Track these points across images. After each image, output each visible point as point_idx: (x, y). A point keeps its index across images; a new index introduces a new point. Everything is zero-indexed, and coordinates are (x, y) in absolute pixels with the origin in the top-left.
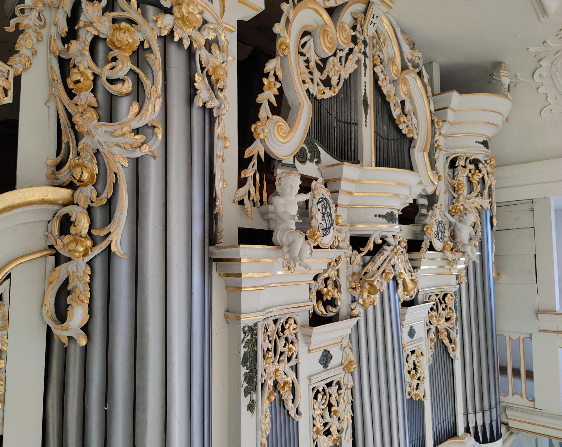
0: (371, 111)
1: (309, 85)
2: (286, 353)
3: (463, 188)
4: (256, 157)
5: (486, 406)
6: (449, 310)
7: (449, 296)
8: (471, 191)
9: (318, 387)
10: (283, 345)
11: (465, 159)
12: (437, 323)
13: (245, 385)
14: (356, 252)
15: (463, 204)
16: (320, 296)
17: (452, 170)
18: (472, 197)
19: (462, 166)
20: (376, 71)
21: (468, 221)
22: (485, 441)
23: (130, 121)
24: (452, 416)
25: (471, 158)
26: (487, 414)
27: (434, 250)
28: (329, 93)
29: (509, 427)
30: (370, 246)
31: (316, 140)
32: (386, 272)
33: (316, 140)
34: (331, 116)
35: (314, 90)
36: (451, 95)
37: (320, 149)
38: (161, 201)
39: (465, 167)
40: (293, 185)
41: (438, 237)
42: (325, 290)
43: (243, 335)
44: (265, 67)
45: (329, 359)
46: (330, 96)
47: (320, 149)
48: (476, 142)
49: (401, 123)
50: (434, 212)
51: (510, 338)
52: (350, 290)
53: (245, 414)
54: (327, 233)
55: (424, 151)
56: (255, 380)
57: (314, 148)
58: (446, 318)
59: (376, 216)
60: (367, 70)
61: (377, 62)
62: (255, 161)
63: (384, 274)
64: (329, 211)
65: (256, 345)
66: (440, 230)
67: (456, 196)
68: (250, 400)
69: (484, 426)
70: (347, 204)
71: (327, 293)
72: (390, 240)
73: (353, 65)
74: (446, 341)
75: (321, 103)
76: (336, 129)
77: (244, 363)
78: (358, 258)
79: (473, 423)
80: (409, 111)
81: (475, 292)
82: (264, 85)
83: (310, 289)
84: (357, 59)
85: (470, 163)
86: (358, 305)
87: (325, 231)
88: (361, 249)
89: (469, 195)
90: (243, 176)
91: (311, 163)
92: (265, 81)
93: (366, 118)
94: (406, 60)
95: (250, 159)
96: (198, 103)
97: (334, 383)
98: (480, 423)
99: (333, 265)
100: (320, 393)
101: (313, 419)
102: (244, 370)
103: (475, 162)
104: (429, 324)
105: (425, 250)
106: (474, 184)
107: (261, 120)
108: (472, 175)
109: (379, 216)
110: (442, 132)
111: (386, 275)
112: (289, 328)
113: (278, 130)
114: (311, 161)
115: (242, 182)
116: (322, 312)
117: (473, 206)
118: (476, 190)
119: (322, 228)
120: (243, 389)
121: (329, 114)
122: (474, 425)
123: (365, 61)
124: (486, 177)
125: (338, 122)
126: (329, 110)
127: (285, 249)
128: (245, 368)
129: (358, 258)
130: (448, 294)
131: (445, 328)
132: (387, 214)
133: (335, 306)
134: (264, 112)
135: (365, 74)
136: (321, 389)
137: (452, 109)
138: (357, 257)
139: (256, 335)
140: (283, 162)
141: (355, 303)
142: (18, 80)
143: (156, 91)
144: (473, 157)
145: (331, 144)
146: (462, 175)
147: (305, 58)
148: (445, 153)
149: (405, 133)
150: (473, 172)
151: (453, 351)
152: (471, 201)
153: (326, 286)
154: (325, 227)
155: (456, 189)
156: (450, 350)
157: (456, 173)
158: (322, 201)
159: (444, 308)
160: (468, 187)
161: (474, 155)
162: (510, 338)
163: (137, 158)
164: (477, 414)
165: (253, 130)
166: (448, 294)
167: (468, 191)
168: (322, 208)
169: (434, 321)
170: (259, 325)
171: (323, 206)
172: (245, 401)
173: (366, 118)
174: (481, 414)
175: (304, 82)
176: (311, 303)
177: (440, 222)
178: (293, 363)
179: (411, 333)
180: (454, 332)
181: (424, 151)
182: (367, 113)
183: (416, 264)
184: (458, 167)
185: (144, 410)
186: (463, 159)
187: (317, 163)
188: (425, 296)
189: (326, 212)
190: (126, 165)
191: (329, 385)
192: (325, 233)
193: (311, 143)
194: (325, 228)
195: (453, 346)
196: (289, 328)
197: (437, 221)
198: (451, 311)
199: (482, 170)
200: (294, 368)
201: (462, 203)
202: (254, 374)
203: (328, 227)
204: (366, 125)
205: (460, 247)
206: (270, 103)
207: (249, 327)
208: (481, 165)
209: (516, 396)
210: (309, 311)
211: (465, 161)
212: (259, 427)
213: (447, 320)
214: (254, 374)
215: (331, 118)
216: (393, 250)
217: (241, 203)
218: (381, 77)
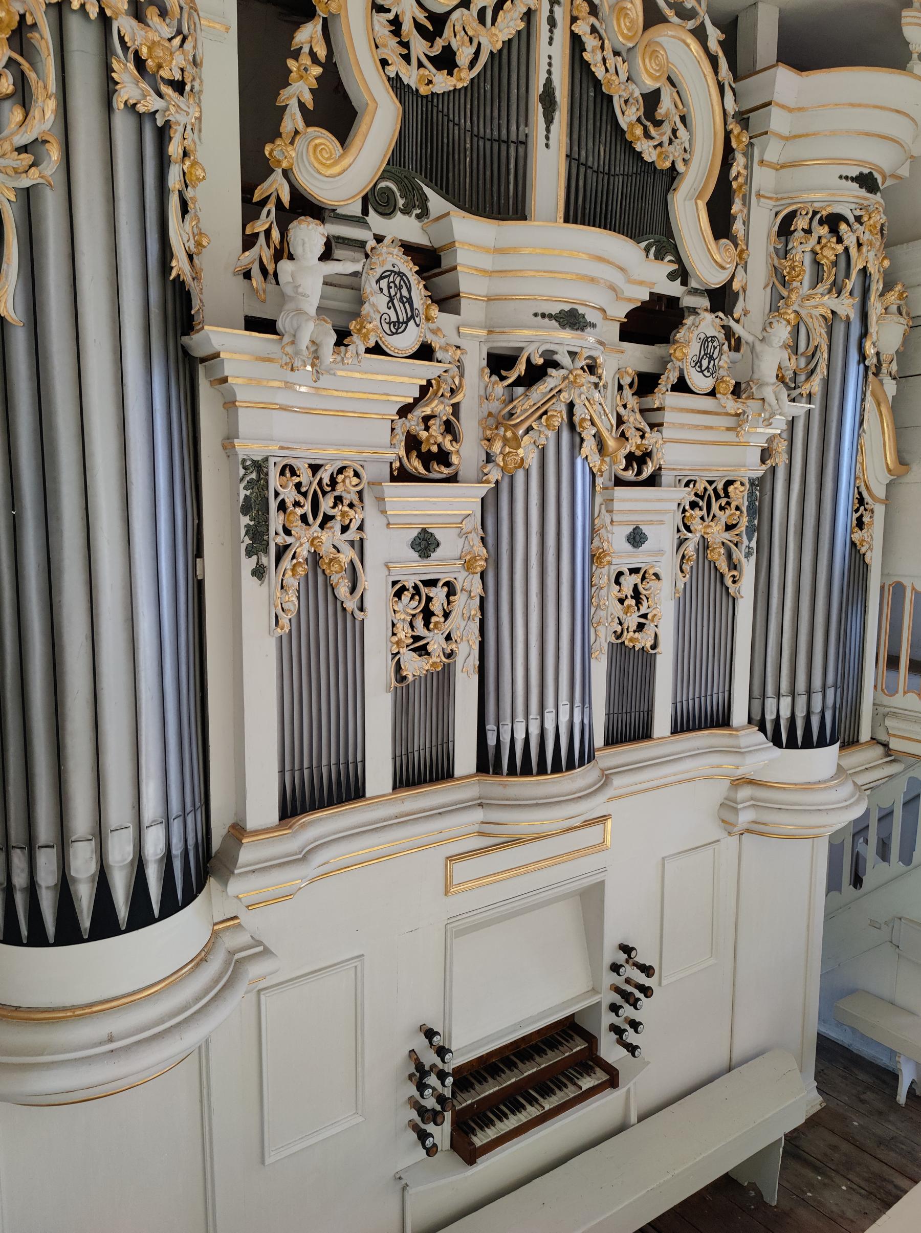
0: (561, 116)
1: (397, 67)
2: (338, 518)
3: (800, 277)
4: (273, 200)
5: (801, 686)
6: (733, 511)
7: (737, 484)
8: (817, 280)
9: (404, 581)
10: (332, 504)
11: (810, 215)
12: (703, 531)
13: (248, 541)
14: (495, 378)
15: (798, 309)
16: (412, 443)
17: (783, 239)
18: (816, 294)
19: (803, 230)
20: (576, 31)
21: (773, 338)
22: (792, 744)
23: (12, 134)
24: (724, 692)
25: (824, 213)
26: (801, 701)
27: (689, 391)
28: (443, 83)
29: (889, 749)
30: (521, 368)
31: (421, 174)
32: (549, 414)
33: (421, 174)
34: (456, 128)
35: (411, 76)
36: (776, 72)
37: (426, 190)
38: (65, 249)
39: (808, 232)
40: (306, 240)
41: (700, 367)
42: (424, 434)
43: (242, 472)
44: (293, 38)
45: (432, 547)
46: (452, 88)
47: (426, 190)
48: (841, 177)
49: (639, 139)
50: (697, 320)
51: (913, 588)
52: (483, 443)
53: (248, 582)
54: (400, 330)
55: (699, 197)
56: (265, 537)
57: (413, 189)
58: (726, 525)
59: (536, 315)
60: (558, 32)
61: (581, 11)
62: (271, 206)
63: (545, 417)
64: (405, 292)
65: (267, 489)
66: (706, 354)
67: (785, 293)
68: (257, 564)
69: (792, 720)
70: (484, 293)
71: (428, 439)
72: (565, 360)
73: (512, 24)
74: (723, 566)
75: (432, 102)
76: (468, 153)
77: (246, 509)
78: (499, 389)
79: (772, 712)
80: (667, 114)
81: (801, 481)
82: (290, 72)
83: (393, 429)
84: (525, 10)
85: (821, 222)
86: (496, 467)
87: (394, 326)
88: (504, 373)
89: (811, 292)
90: (248, 232)
91: (406, 217)
92: (292, 64)
93: (548, 130)
95: (264, 202)
96: (118, 104)
97: (440, 584)
98: (785, 713)
99: (442, 395)
100: (408, 590)
101: (393, 625)
102: (245, 520)
103: (833, 222)
104: (682, 529)
105: (665, 389)
106: (825, 268)
107: (284, 135)
108: (822, 249)
109: (543, 316)
110: (766, 158)
111: (547, 419)
112: (344, 481)
113: (315, 151)
114: (406, 211)
115: (249, 242)
116: (416, 469)
117: (816, 312)
118: (828, 278)
119: (387, 321)
120: (243, 547)
121: (451, 124)
122: (774, 716)
123: (551, 11)
124: (853, 251)
125: (475, 139)
126: (451, 116)
127: (286, 339)
128: (248, 517)
129: (499, 389)
130: (735, 481)
131: (723, 543)
132: (560, 313)
133: (448, 464)
134: (293, 119)
135: (551, 39)
136: (409, 585)
137: (783, 107)
138: (496, 386)
139: (267, 474)
140: (339, 211)
141: (490, 465)
143: (45, 87)
144: (830, 210)
145: (456, 183)
146: (801, 249)
147: (391, 16)
148: (774, 203)
149: (650, 160)
150: (824, 241)
151: (734, 582)
152: (812, 302)
153: (427, 429)
154: (394, 319)
155: (787, 278)
156: (728, 581)
157: (790, 247)
158: (389, 276)
159: (723, 505)
160: (811, 275)
161: (829, 205)
162: (913, 588)
163: (28, 189)
164: (782, 699)
165: (267, 153)
166: (735, 481)
167: (811, 282)
168: (389, 288)
169: (696, 525)
170: (272, 461)
171: (392, 285)
172: (248, 564)
173: (548, 130)
174: (789, 699)
175: (384, 63)
176: (396, 450)
177: (709, 339)
178: (352, 534)
179: (634, 538)
180: (741, 552)
181: (699, 197)
182: (553, 119)
183: (655, 418)
184: (795, 234)
185: (59, 519)
186: (807, 214)
187: (418, 217)
188: (679, 480)
189: (398, 295)
190: (13, 199)
192: (394, 331)
193: (405, 180)
194: (394, 323)
195: (735, 573)
196: (344, 481)
197: (703, 336)
198: (738, 513)
199: (845, 237)
200: (357, 545)
201: (796, 308)
202: (263, 529)
203: (401, 320)
204: (547, 146)
205: (754, 390)
206: (302, 106)
207: (253, 461)
208: (843, 227)
209: (910, 695)
210: (391, 463)
211: (811, 219)
212: (272, 602)
213: (729, 528)
214: (263, 529)
215: (456, 132)
216: (565, 378)
217: (247, 275)
218: (590, 42)
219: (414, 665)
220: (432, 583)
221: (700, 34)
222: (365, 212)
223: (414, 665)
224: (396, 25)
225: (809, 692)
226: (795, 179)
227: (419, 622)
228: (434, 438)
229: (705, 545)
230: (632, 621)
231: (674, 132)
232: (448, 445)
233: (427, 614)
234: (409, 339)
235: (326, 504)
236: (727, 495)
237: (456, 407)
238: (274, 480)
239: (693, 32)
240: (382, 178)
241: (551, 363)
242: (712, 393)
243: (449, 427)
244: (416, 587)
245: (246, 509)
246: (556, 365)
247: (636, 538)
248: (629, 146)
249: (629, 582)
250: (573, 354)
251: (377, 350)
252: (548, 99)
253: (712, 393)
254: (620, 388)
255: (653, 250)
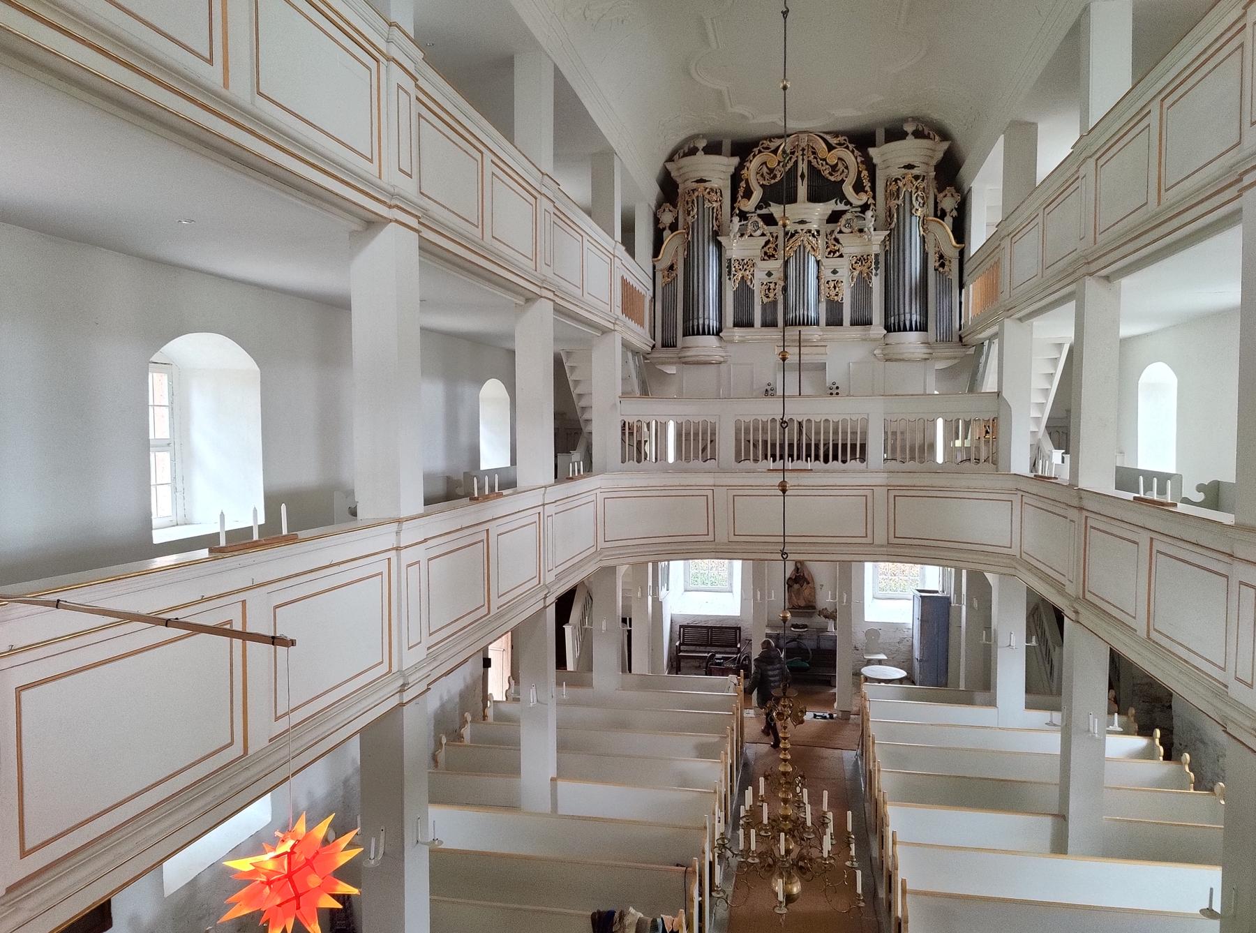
5: (896, 313)
16: (766, 253)
26: (897, 317)
28: (773, 181)
35: (766, 183)
77: (727, 267)
94: (834, 145)
114: (766, 208)
142: (678, 211)
191: (771, 283)
219: (765, 300)
220: (771, 283)
221: (847, 148)
222: (756, 210)
223: (765, 300)
224: (762, 175)
225: (899, 315)
226: (889, 171)
227: (767, 291)
228: (771, 252)
229: (861, 272)
230: (833, 293)
231: (843, 171)
232: (774, 252)
233: (769, 289)
234: (759, 232)
235: (745, 267)
236: (868, 259)
237: (777, 245)
238: (733, 262)
239: (845, 148)
240: (759, 202)
241: (796, 232)
242: (852, 232)
243: (775, 250)
244: (767, 284)
245: (727, 267)
246: (798, 233)
247: (835, 272)
248: (827, 179)
249: (832, 284)
250: (802, 230)
251: (751, 236)
252: (802, 176)
253: (852, 232)
254: (827, 235)
255: (838, 201)
